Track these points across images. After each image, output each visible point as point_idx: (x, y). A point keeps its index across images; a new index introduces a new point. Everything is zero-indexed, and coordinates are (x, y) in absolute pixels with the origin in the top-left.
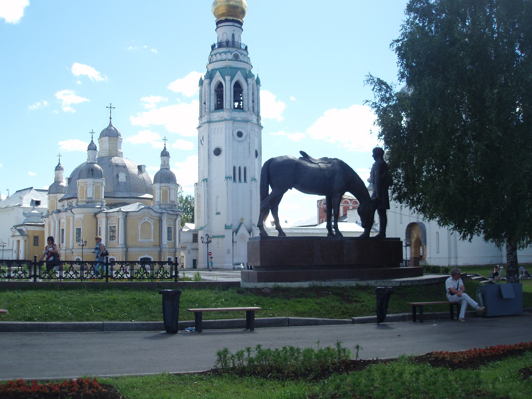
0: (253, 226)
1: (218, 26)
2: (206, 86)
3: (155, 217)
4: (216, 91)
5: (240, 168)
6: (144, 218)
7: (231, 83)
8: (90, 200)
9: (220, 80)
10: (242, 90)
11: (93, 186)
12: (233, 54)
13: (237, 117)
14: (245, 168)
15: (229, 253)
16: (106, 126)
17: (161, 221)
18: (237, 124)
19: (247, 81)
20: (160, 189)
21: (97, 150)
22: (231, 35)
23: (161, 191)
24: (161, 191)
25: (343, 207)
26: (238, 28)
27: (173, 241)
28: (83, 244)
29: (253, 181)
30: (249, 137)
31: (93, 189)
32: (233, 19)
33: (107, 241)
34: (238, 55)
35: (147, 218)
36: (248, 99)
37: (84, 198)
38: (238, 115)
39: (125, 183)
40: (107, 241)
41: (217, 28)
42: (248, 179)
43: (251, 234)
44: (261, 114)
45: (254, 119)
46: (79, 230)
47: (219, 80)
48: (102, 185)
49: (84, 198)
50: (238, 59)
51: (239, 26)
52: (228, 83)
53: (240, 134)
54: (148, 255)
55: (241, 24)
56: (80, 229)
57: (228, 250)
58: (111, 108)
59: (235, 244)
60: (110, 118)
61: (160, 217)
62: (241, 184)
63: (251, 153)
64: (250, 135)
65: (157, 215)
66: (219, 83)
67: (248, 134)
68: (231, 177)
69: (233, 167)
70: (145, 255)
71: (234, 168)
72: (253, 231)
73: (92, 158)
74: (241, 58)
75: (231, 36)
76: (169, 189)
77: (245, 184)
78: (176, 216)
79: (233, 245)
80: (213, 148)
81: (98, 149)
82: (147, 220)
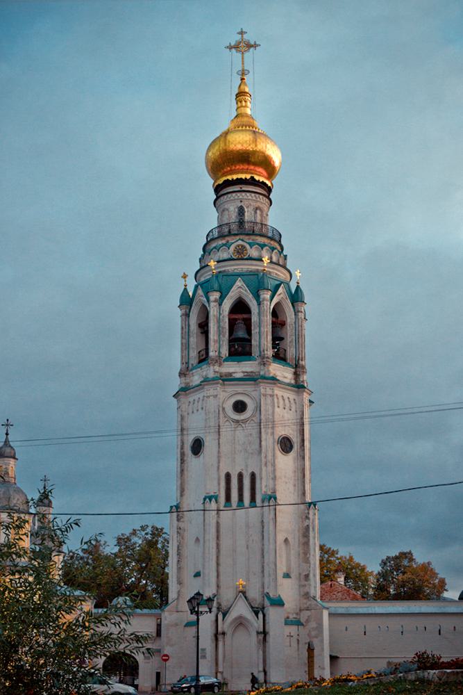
0: (265, 598)
5: (240, 476)
12: (232, 248)
13: (234, 373)
14: (253, 476)
18: (231, 389)
19: (257, 297)
32: (239, 177)
36: (259, 333)
41: (218, 198)
43: (261, 615)
44: (308, 363)
62: (241, 512)
67: (259, 402)
71: (228, 476)
79: (217, 639)
80: (189, 440)
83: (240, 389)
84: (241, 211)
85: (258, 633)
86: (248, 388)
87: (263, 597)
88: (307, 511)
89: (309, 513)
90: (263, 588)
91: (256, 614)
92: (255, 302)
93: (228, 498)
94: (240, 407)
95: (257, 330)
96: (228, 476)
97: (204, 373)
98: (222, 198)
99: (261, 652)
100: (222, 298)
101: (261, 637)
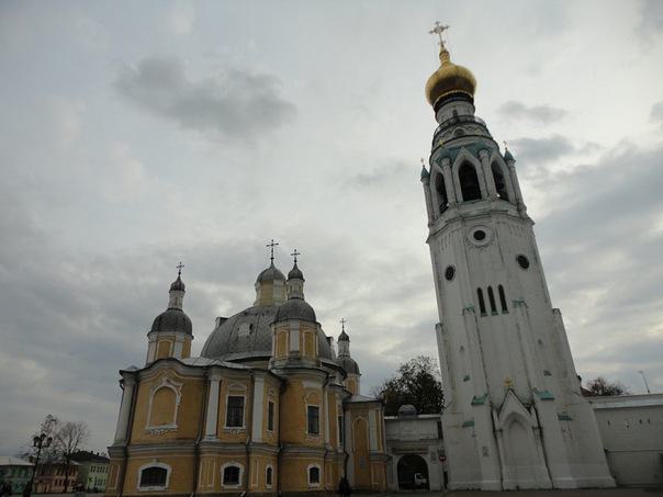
5: (490, 290)
14: (501, 289)
15: (486, 454)
16: (268, 266)
18: (469, 224)
19: (478, 157)
35: (164, 379)
38: (473, 208)
43: (533, 411)
52: (447, 168)
53: (480, 236)
59: (499, 434)
71: (480, 291)
79: (495, 437)
82: (164, 384)
83: (478, 222)
84: (455, 112)
86: (485, 221)
91: (529, 409)
93: (483, 309)
96: (480, 291)
99: (540, 448)
101: (537, 432)
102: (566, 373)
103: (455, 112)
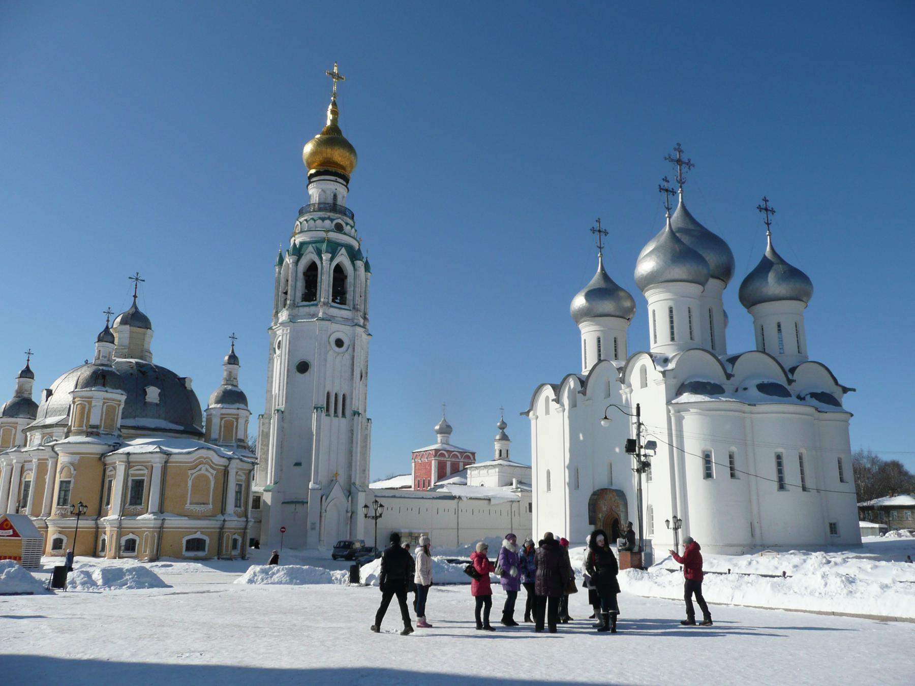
1: (311, 180)
2: (291, 266)
3: (216, 465)
4: (305, 274)
5: (336, 394)
6: (200, 467)
7: (330, 264)
8: (95, 430)
9: (313, 259)
10: (346, 277)
11: (103, 405)
15: (313, 529)
17: (226, 473)
18: (334, 327)
20: (222, 419)
21: (115, 343)
22: (332, 195)
23: (223, 422)
24: (223, 422)
25: (451, 463)
26: (343, 187)
27: (243, 508)
28: (80, 512)
29: (356, 416)
30: (354, 348)
31: (102, 411)
33: (124, 506)
34: (341, 225)
36: (354, 291)
37: (82, 427)
39: (157, 405)
40: (124, 506)
42: (348, 412)
43: (350, 498)
45: (361, 321)
46: (64, 485)
47: (312, 260)
48: (119, 405)
49: (82, 427)
50: (342, 231)
51: (345, 183)
52: (326, 263)
54: (202, 533)
55: (347, 180)
56: (69, 482)
57: (313, 524)
58: (137, 279)
60: (135, 296)
61: (225, 466)
63: (355, 373)
64: (354, 346)
65: (223, 462)
66: (311, 263)
68: (324, 408)
69: (794, 322)
70: (196, 532)
71: (328, 395)
72: (352, 494)
73: (105, 357)
74: (347, 229)
75: (332, 197)
76: (237, 419)
77: (344, 419)
78: (251, 465)
80: (297, 361)
81: (116, 341)
82: (203, 471)
85: (347, 512)
87: (350, 485)
88: (366, 424)
89: (368, 426)
90: (351, 479)
92: (352, 268)
93: (328, 410)
94: (339, 343)
95: (352, 289)
96: (328, 395)
97: (312, 313)
98: (313, 184)
100: (332, 259)
101: (349, 514)
102: (364, 470)
103: (335, 196)
